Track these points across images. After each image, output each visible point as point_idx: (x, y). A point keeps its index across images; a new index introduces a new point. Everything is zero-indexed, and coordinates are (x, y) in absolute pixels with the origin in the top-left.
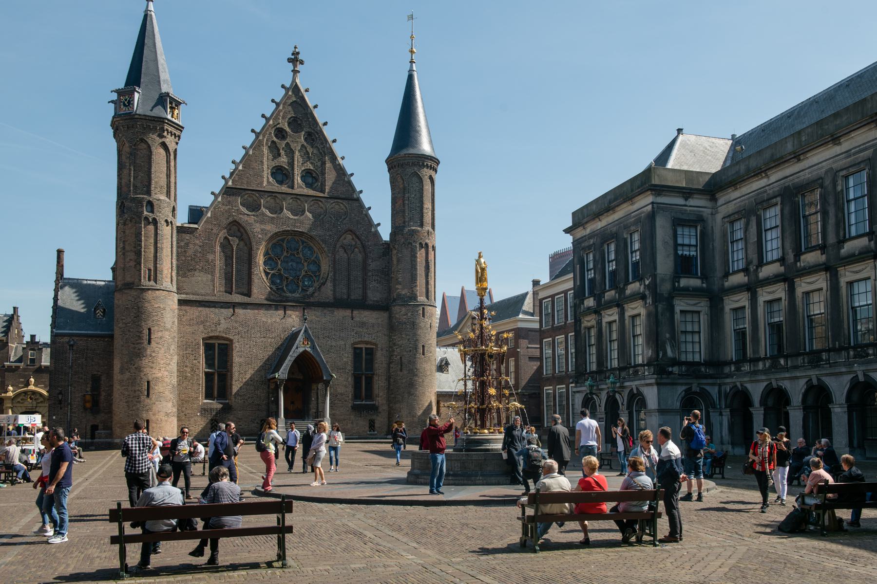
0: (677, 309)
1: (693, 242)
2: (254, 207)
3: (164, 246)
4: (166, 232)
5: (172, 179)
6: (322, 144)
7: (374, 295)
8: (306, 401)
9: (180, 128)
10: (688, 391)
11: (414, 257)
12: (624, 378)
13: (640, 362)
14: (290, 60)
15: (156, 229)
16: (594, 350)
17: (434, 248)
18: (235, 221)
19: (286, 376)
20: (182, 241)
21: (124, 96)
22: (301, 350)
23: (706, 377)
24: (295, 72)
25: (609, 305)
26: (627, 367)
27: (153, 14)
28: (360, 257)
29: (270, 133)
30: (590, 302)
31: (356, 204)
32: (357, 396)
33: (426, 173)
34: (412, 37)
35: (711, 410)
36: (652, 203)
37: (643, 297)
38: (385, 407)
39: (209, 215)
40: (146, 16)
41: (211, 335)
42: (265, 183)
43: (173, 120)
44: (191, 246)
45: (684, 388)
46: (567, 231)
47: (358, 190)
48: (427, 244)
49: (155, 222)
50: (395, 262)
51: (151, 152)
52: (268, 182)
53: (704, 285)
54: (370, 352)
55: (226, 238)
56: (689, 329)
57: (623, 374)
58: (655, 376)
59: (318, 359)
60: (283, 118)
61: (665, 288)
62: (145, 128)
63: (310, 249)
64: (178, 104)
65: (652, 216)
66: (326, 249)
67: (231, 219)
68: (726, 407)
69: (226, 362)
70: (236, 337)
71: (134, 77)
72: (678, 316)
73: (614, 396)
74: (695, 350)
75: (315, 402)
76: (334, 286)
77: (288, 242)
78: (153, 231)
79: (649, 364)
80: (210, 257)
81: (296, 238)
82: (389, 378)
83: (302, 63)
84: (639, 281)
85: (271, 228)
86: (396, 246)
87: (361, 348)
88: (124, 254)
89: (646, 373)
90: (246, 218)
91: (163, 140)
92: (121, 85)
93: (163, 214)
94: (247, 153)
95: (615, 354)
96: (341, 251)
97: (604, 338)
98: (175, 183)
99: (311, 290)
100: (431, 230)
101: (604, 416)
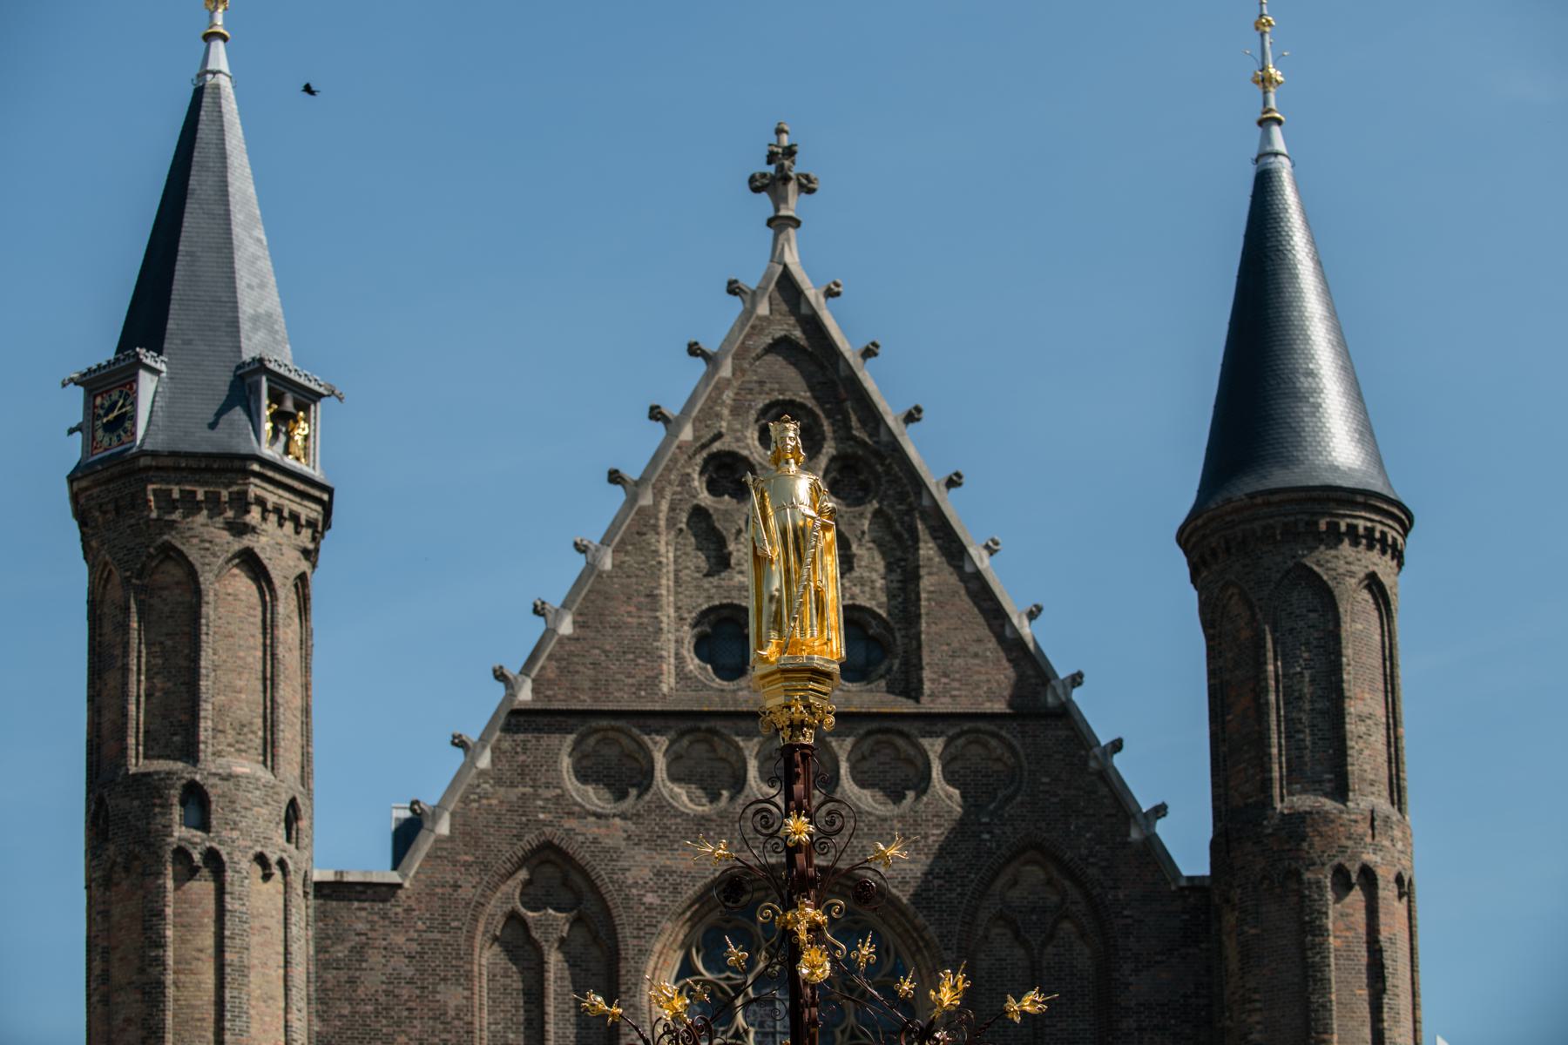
2: (623, 776)
3: (255, 957)
4: (258, 899)
5: (289, 693)
6: (902, 497)
9: (322, 495)
11: (1310, 929)
14: (757, 185)
15: (220, 892)
17: (1404, 886)
18: (548, 846)
20: (340, 939)
21: (107, 390)
24: (779, 224)
27: (224, 81)
29: (685, 479)
34: (1260, 26)
39: (444, 828)
40: (199, 93)
42: (668, 683)
43: (289, 461)
44: (375, 958)
47: (1063, 672)
49: (214, 861)
50: (1233, 963)
51: (197, 592)
52: (682, 675)
55: (513, 918)
60: (736, 411)
62: (172, 505)
64: (307, 398)
66: (932, 932)
67: (531, 839)
71: (147, 321)
78: (210, 904)
80: (452, 997)
86: (1236, 894)
88: (105, 1000)
90: (592, 828)
91: (247, 541)
92: (104, 351)
93: (248, 828)
94: (591, 567)
98: (306, 711)
100: (1383, 805)
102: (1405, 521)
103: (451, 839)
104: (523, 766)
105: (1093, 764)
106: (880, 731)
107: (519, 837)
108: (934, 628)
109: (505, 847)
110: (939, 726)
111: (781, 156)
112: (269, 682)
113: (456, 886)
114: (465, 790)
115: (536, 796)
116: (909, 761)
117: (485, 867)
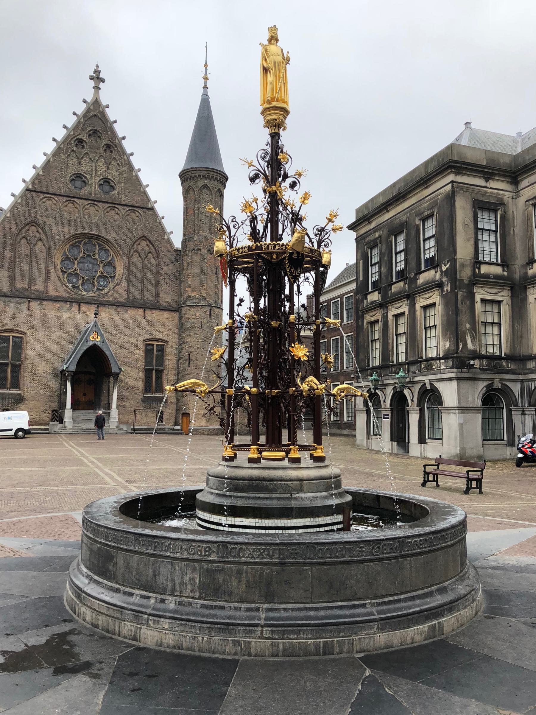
0: (478, 298)
1: (493, 228)
7: (167, 296)
8: (98, 393)
10: (490, 388)
12: (414, 373)
13: (434, 355)
14: (91, 78)
16: (377, 345)
19: (73, 368)
22: (91, 344)
23: (508, 372)
24: (97, 88)
25: (397, 298)
26: (418, 361)
28: (153, 262)
29: (70, 143)
30: (375, 297)
32: (147, 388)
33: (214, 185)
34: (206, 65)
35: (513, 408)
36: (452, 182)
37: (440, 285)
39: (8, 215)
41: (5, 328)
45: (485, 383)
46: (352, 227)
53: (505, 273)
54: (161, 349)
56: (489, 320)
57: (413, 368)
58: (455, 370)
61: (465, 274)
63: (106, 250)
65: (451, 198)
67: (30, 219)
68: (530, 405)
69: (20, 354)
70: (31, 331)
72: (478, 305)
73: (402, 392)
74: (496, 342)
75: (107, 395)
76: (128, 287)
77: (85, 244)
79: (446, 357)
81: (94, 241)
83: (103, 81)
84: (434, 268)
85: (68, 231)
87: (153, 345)
89: (443, 367)
90: (45, 219)
95: (403, 349)
96: (136, 255)
97: (390, 332)
99: (106, 290)
101: (389, 413)
102: (227, 179)
103: (10, 217)
104: (29, 203)
105: (158, 220)
106: (112, 207)
107: (27, 219)
108: (126, 186)
109: (23, 221)
110: (125, 207)
111: (97, 72)
113: (10, 229)
114: (14, 207)
115: (31, 210)
116: (118, 214)
117: (18, 225)
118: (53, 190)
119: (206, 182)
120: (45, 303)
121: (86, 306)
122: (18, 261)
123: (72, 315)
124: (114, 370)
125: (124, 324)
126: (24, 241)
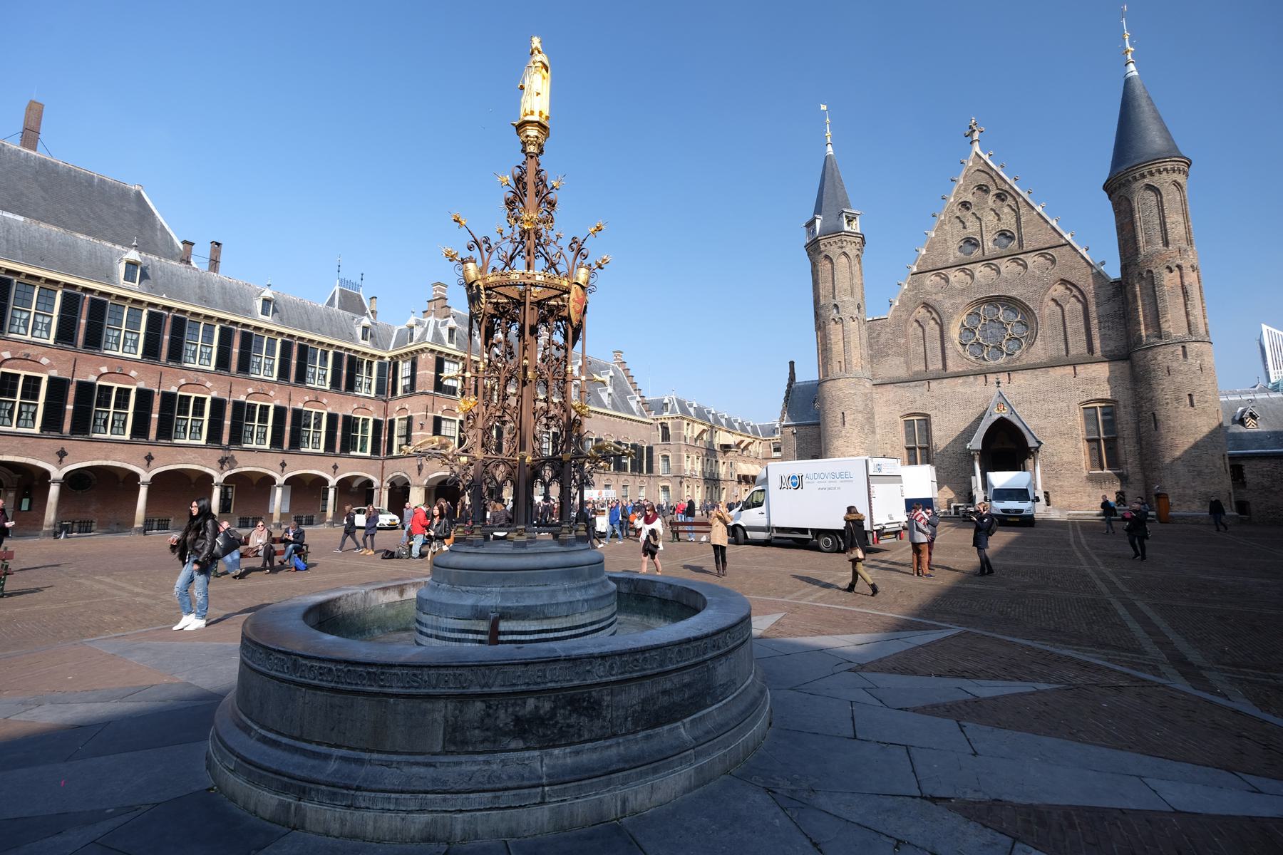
5: (857, 281)
22: (996, 417)
28: (1080, 307)
31: (1068, 248)
38: (1139, 477)
48: (1179, 267)
59: (1019, 425)
82: (1139, 440)
92: (811, 217)
93: (849, 310)
100: (1184, 245)
112: (851, 279)
118: (940, 266)
119: (1146, 181)
120: (945, 381)
121: (994, 376)
122: (912, 345)
123: (978, 389)
124: (1032, 443)
125: (1046, 388)
126: (915, 325)
